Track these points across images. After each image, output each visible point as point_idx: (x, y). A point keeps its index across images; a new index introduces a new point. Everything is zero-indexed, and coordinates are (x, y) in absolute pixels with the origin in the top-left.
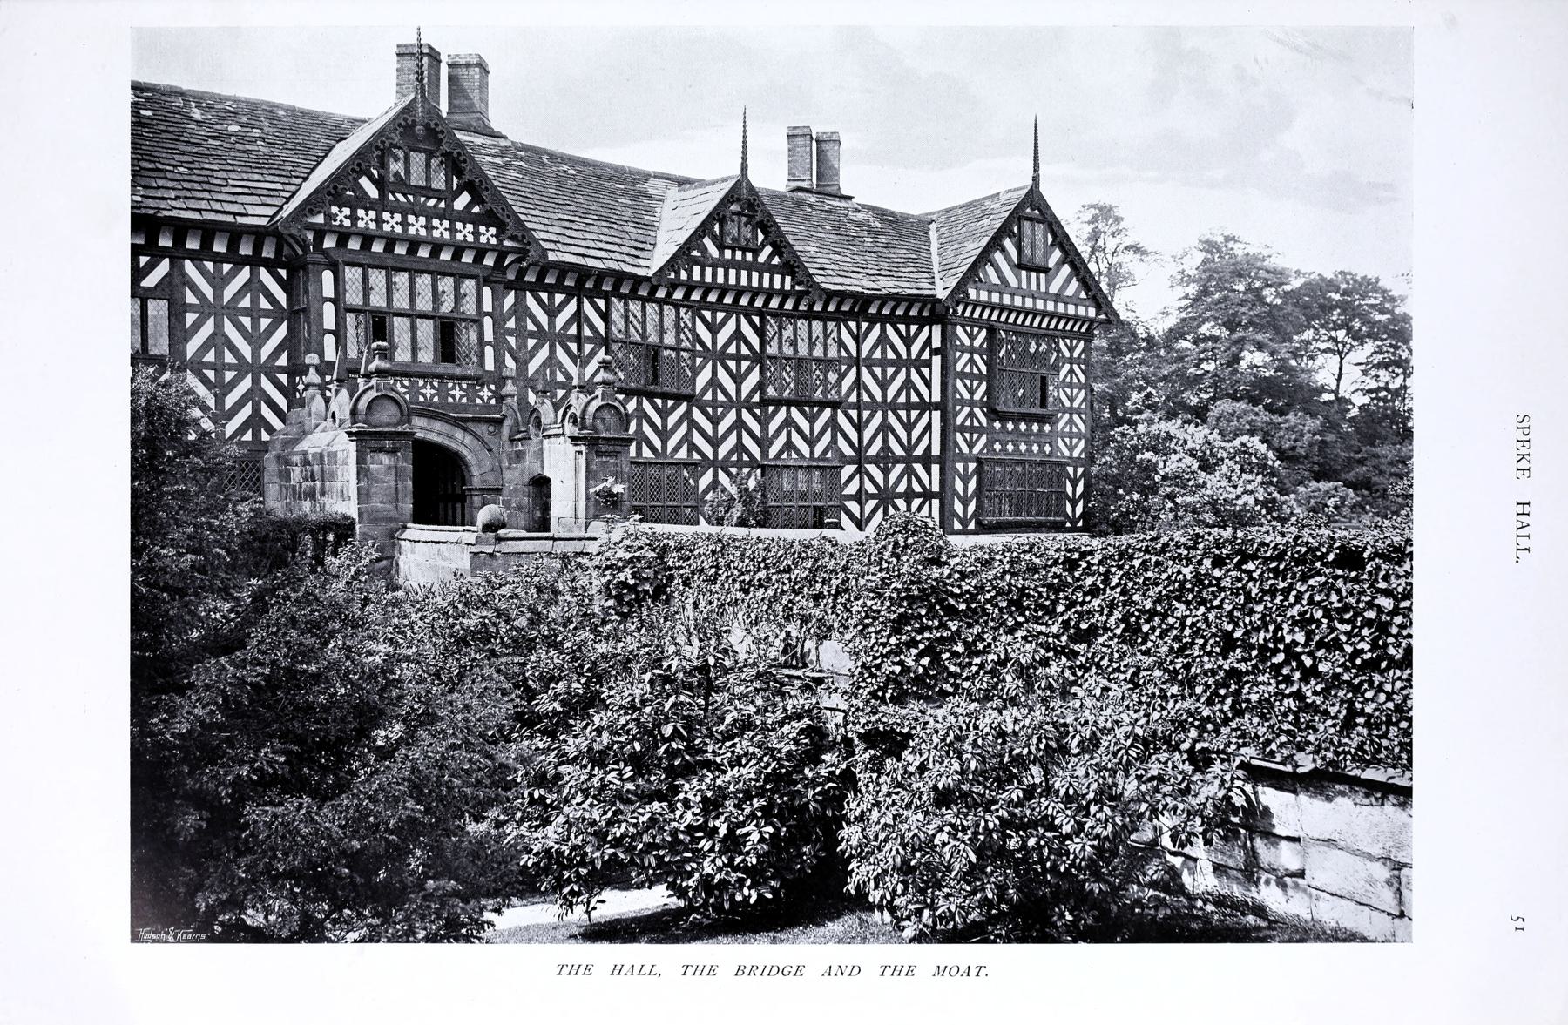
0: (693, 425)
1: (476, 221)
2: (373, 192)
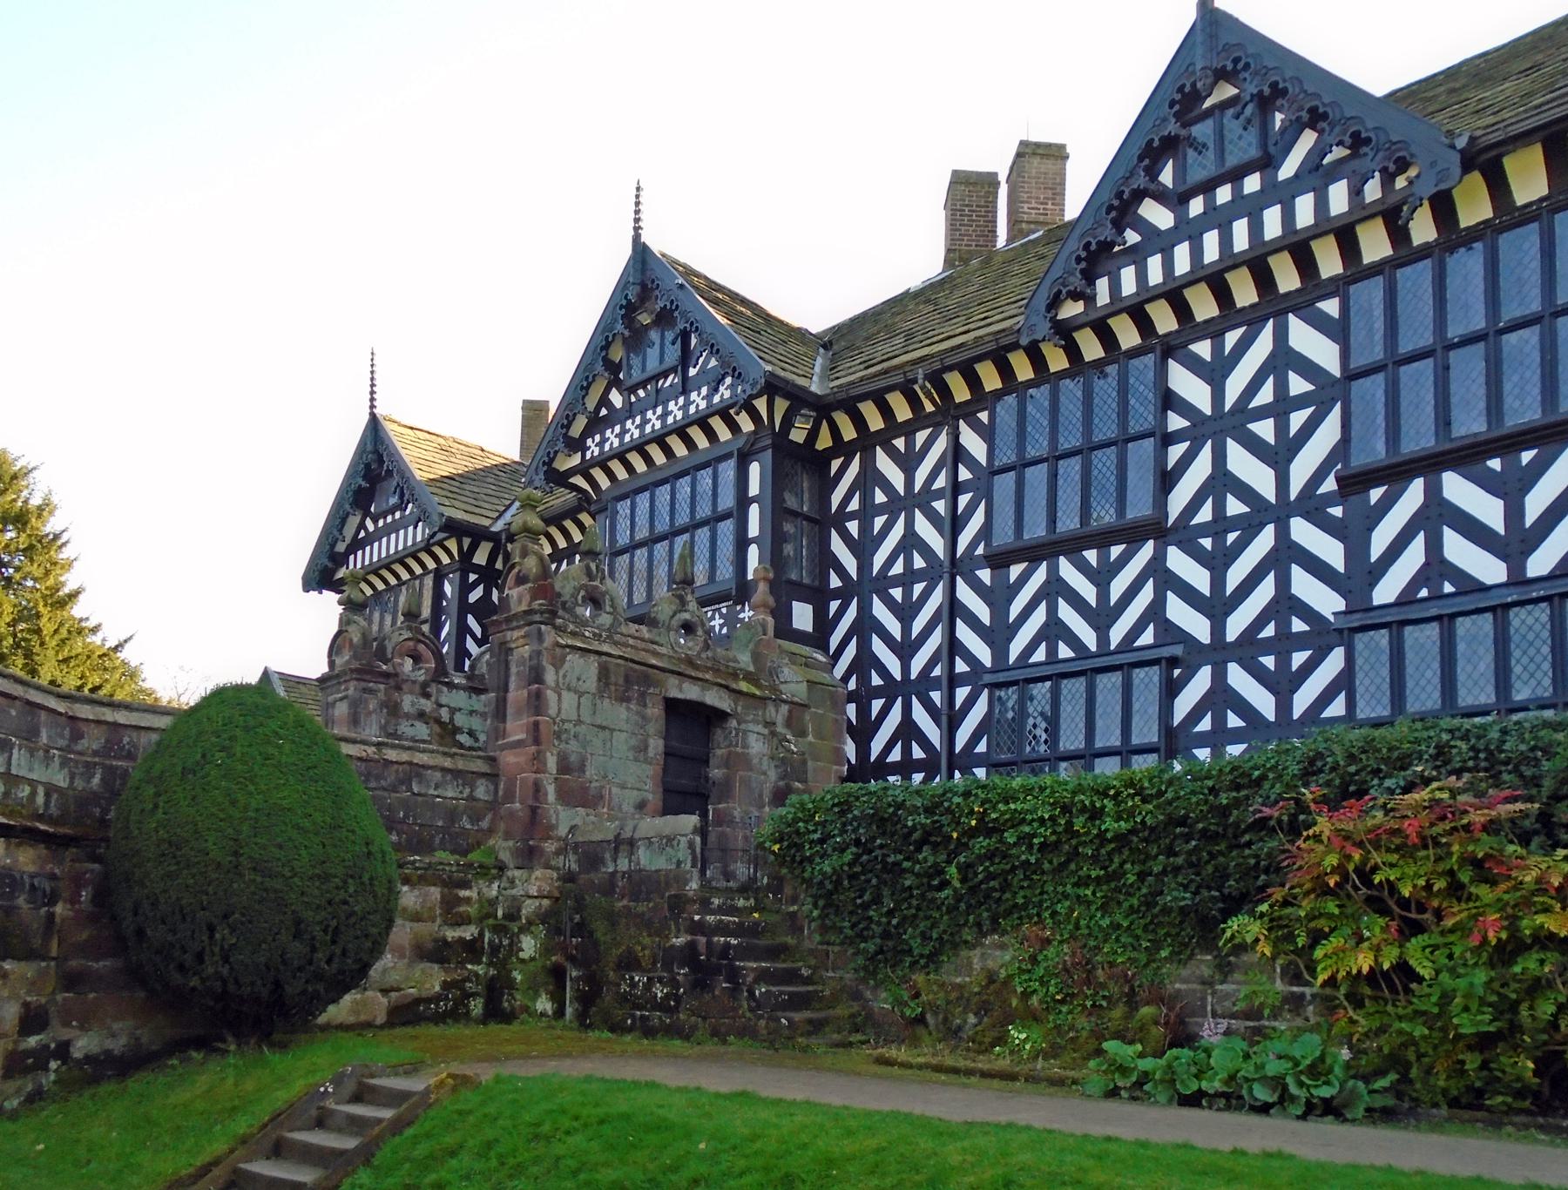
0: (1168, 582)
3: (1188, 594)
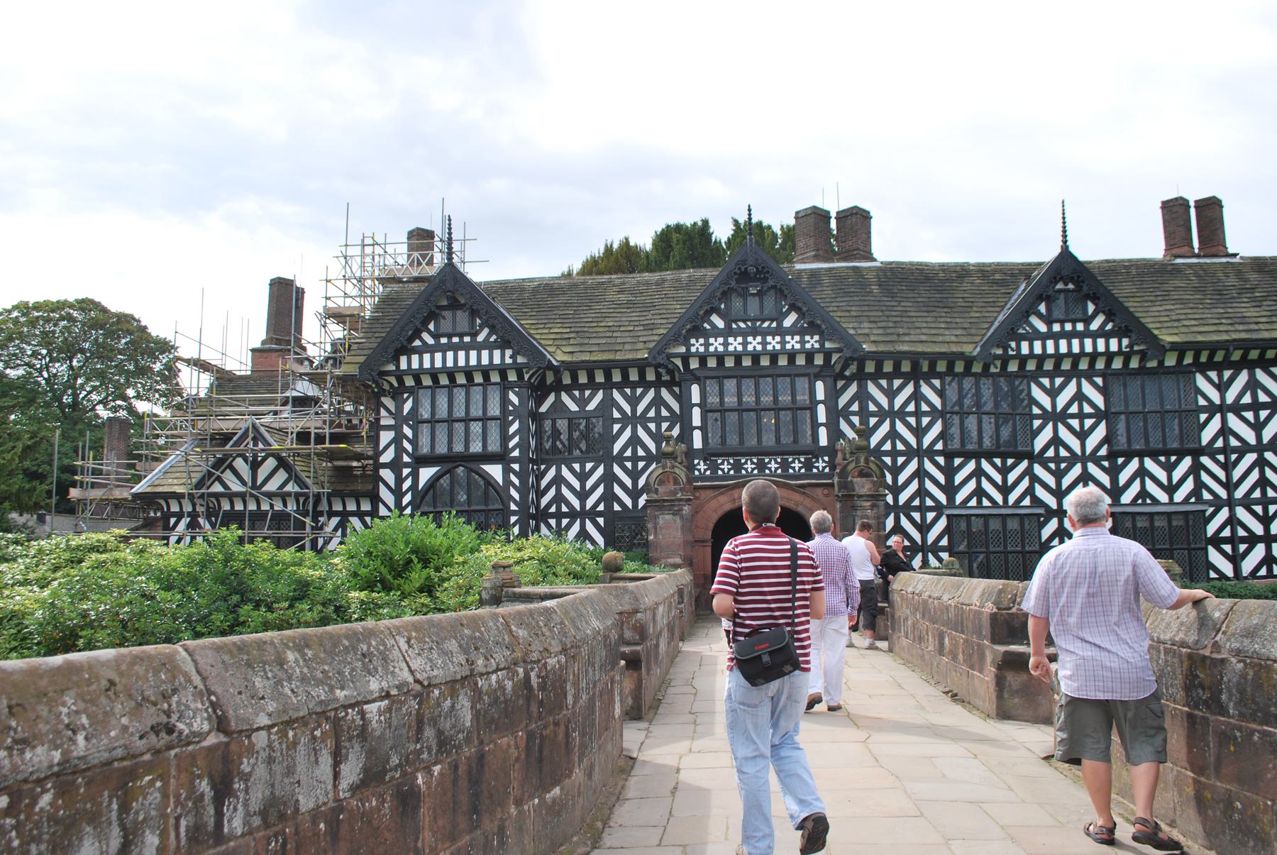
0: (1035, 479)
1: (802, 333)
2: (720, 323)
3: (1045, 486)
